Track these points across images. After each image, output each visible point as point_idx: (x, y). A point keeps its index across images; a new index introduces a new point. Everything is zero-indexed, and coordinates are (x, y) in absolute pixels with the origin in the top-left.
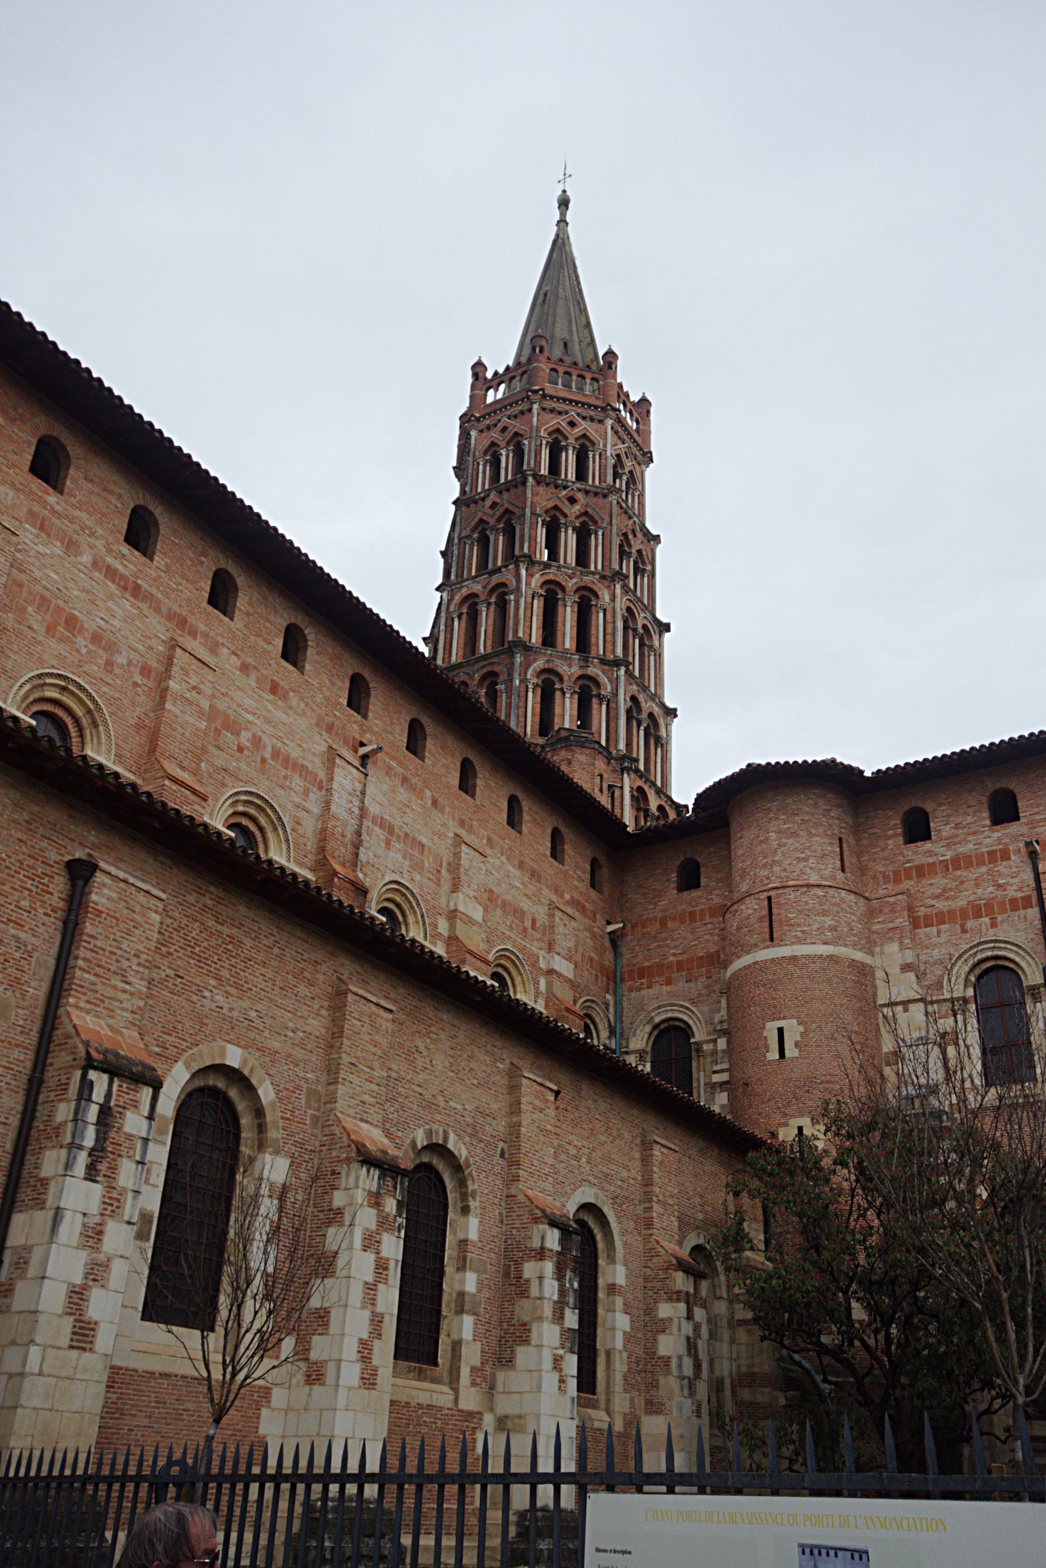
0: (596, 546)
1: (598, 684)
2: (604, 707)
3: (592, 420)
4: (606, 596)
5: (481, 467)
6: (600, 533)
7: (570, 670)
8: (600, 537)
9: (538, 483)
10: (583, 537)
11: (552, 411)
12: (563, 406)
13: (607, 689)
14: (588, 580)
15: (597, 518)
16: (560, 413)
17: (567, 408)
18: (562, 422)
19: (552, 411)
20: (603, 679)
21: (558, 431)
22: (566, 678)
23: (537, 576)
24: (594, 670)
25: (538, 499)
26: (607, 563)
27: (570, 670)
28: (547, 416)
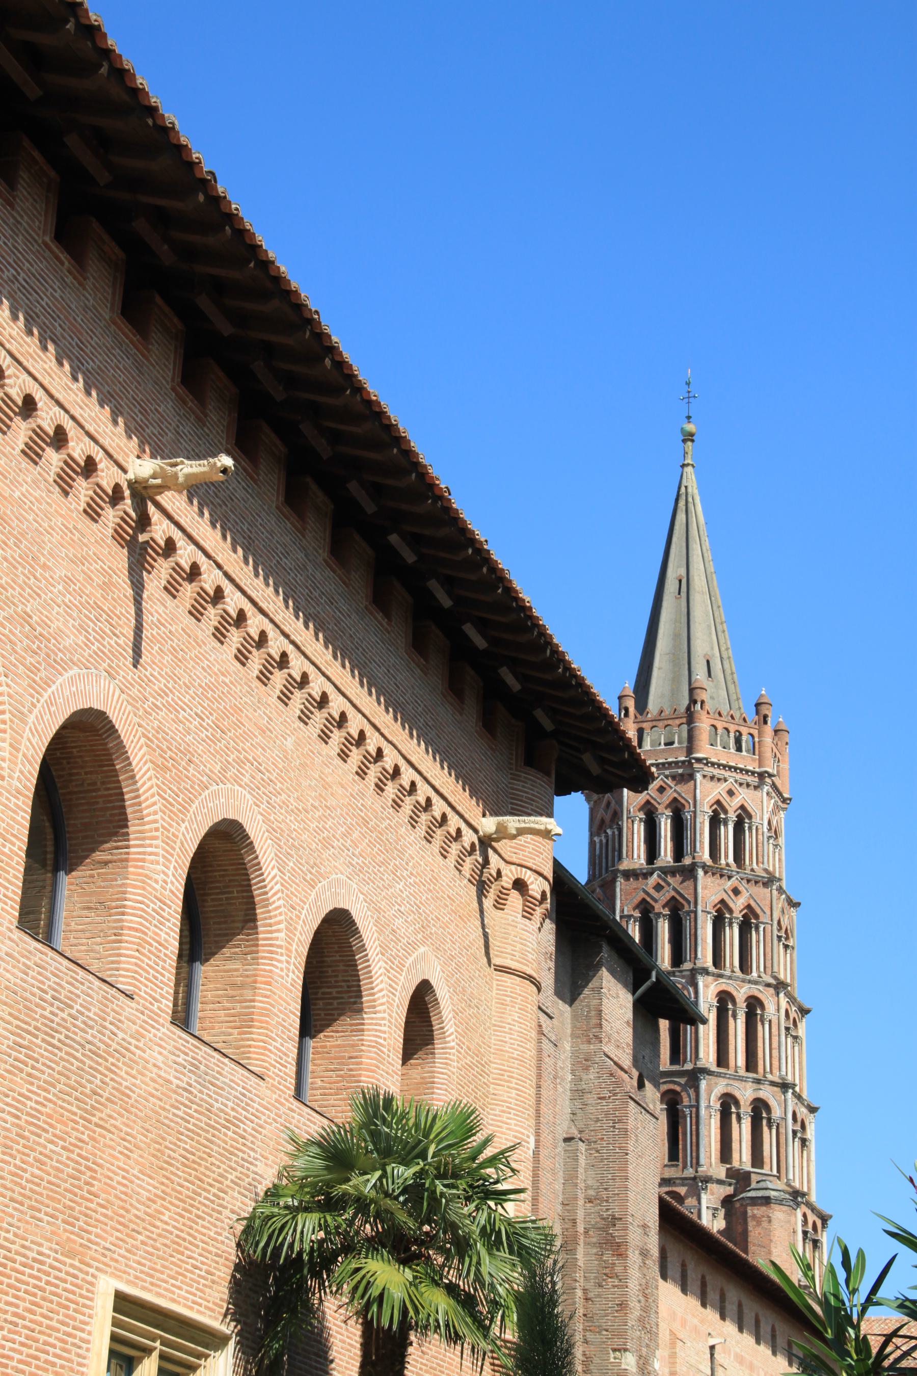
0: (758, 942)
1: (768, 1108)
2: (774, 1131)
3: (748, 785)
4: (770, 1007)
5: (636, 826)
6: (761, 929)
7: (746, 1094)
8: (762, 933)
9: (706, 873)
10: (746, 927)
11: (712, 778)
12: (723, 772)
13: (777, 1113)
14: (755, 990)
15: (758, 911)
16: (719, 780)
17: (727, 774)
18: (722, 788)
19: (712, 778)
20: (772, 1103)
21: (718, 802)
22: (742, 1103)
23: (712, 987)
24: (767, 1093)
25: (709, 891)
26: (769, 965)
27: (746, 1094)
28: (709, 784)
